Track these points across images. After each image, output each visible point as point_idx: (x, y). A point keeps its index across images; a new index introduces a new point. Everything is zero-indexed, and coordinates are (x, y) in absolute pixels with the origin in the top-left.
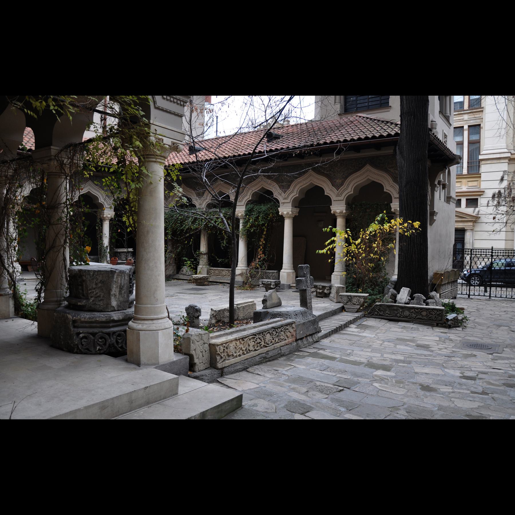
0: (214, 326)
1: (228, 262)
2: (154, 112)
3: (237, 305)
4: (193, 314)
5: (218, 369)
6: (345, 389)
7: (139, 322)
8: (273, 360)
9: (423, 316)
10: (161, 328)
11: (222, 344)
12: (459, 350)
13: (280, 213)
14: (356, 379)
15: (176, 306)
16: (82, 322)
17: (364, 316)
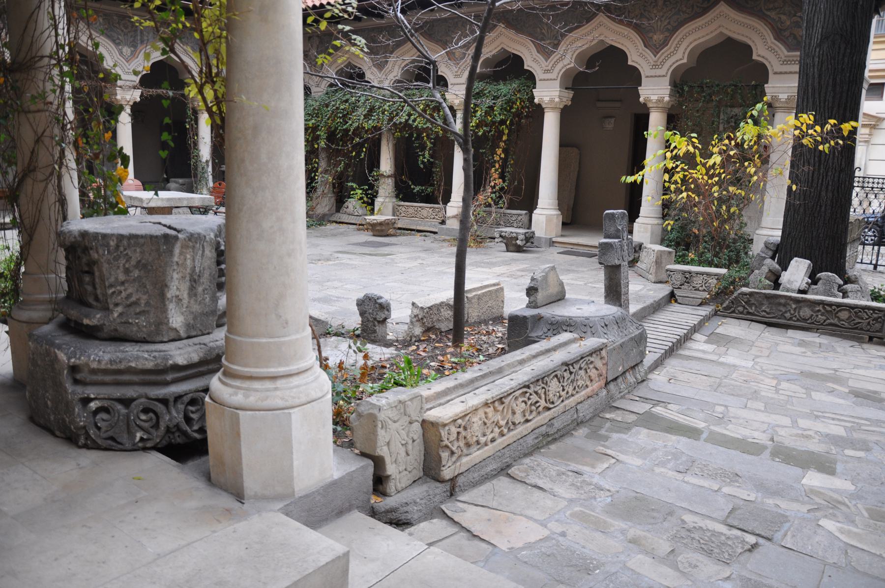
0: (420, 341)
1: (433, 192)
4: (373, 312)
7: (237, 383)
9: (840, 320)
10: (297, 402)
13: (536, 101)
14: (770, 501)
15: (336, 284)
16: (94, 372)
17: (716, 313)
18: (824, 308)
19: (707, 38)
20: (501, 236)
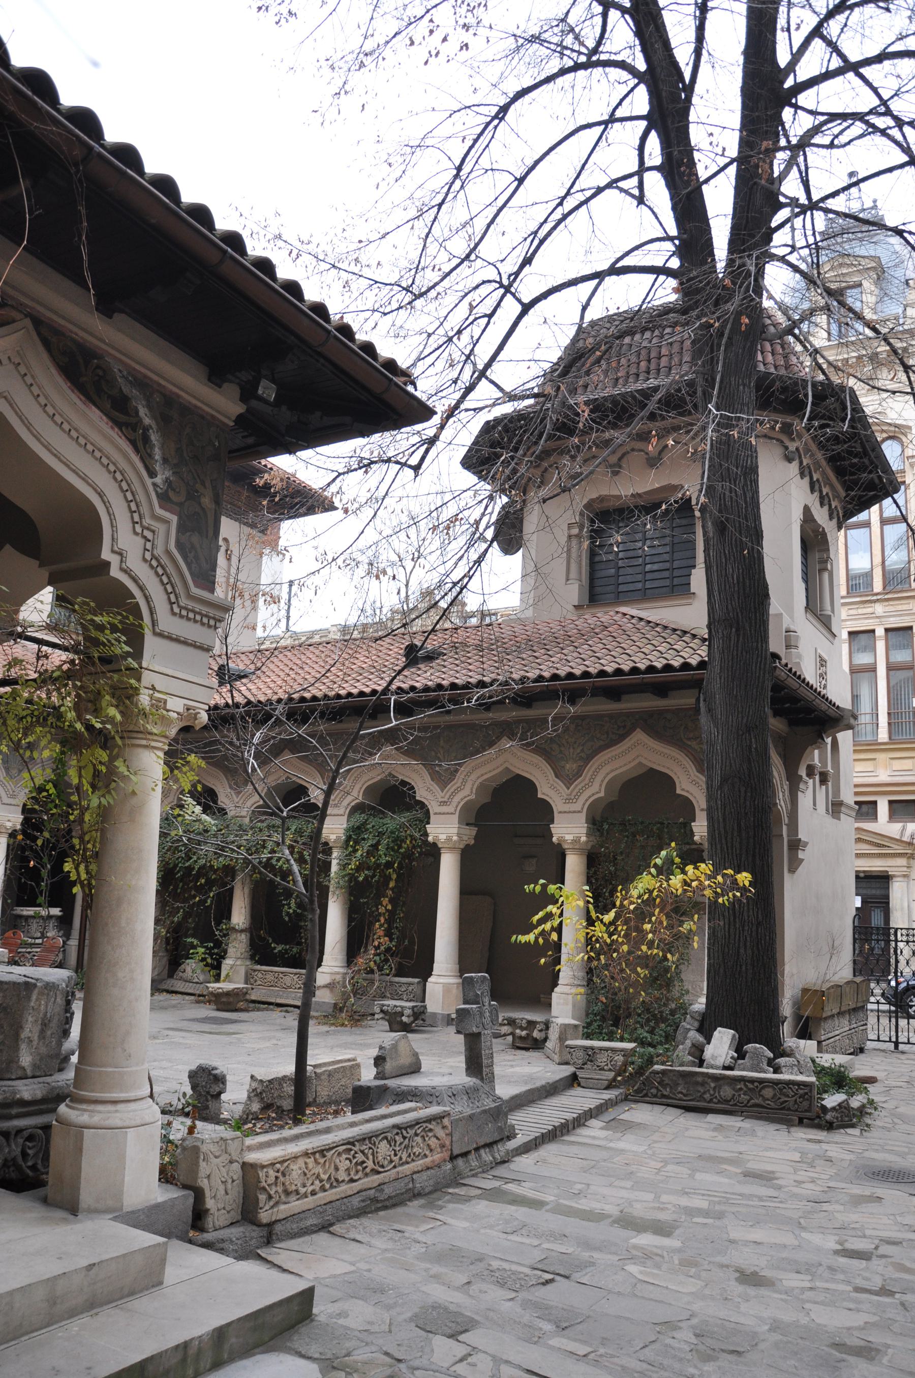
0: (257, 1119)
1: (300, 953)
2: (151, 643)
3: (315, 1066)
5: (259, 1225)
6: (558, 1278)
7: (84, 1106)
8: (394, 1205)
9: (765, 1099)
10: (133, 1123)
11: (273, 1164)
12: (843, 1185)
13: (430, 839)
15: (165, 1064)
17: (626, 1099)
18: (746, 1086)
19: (628, 767)
20: (382, 1011)
